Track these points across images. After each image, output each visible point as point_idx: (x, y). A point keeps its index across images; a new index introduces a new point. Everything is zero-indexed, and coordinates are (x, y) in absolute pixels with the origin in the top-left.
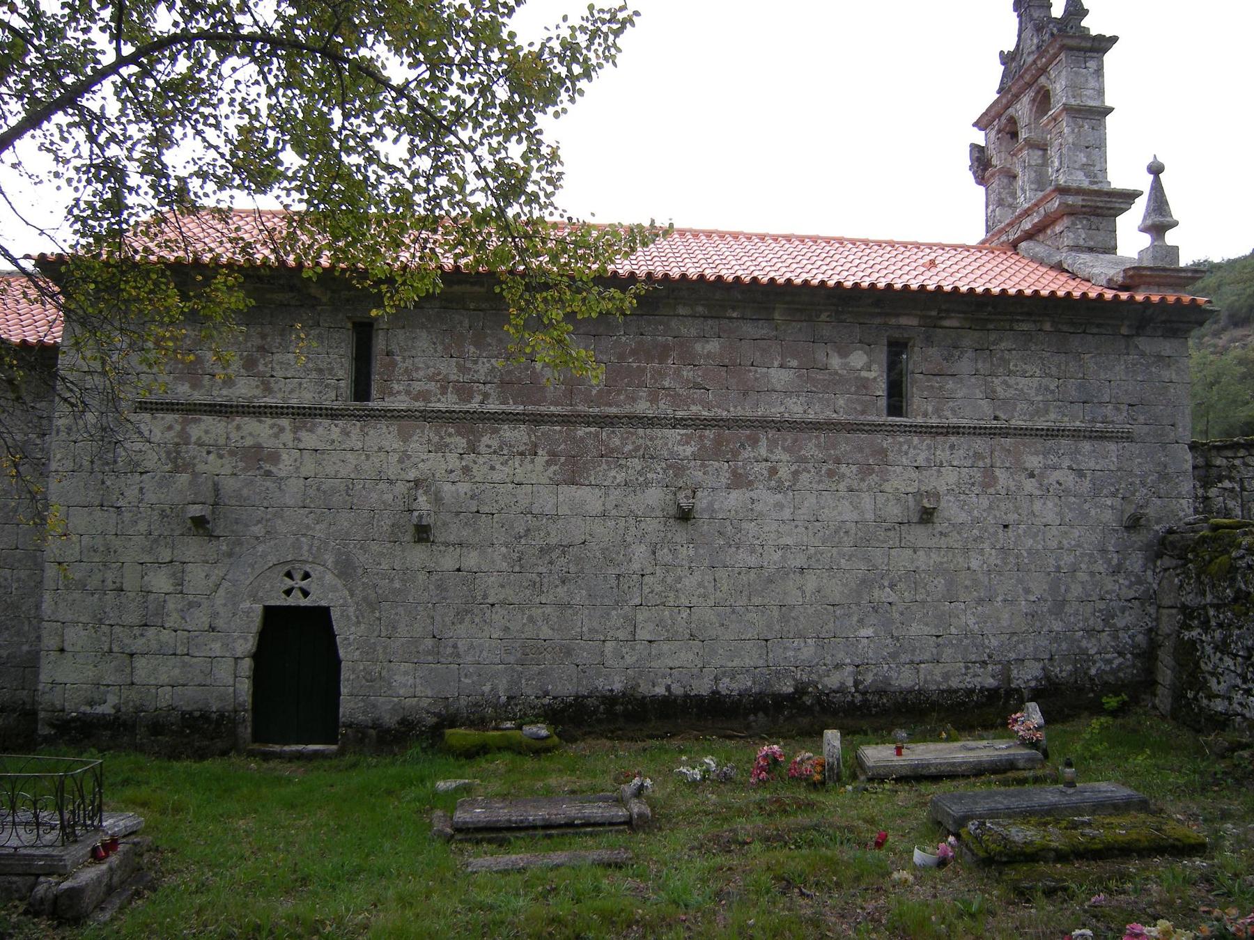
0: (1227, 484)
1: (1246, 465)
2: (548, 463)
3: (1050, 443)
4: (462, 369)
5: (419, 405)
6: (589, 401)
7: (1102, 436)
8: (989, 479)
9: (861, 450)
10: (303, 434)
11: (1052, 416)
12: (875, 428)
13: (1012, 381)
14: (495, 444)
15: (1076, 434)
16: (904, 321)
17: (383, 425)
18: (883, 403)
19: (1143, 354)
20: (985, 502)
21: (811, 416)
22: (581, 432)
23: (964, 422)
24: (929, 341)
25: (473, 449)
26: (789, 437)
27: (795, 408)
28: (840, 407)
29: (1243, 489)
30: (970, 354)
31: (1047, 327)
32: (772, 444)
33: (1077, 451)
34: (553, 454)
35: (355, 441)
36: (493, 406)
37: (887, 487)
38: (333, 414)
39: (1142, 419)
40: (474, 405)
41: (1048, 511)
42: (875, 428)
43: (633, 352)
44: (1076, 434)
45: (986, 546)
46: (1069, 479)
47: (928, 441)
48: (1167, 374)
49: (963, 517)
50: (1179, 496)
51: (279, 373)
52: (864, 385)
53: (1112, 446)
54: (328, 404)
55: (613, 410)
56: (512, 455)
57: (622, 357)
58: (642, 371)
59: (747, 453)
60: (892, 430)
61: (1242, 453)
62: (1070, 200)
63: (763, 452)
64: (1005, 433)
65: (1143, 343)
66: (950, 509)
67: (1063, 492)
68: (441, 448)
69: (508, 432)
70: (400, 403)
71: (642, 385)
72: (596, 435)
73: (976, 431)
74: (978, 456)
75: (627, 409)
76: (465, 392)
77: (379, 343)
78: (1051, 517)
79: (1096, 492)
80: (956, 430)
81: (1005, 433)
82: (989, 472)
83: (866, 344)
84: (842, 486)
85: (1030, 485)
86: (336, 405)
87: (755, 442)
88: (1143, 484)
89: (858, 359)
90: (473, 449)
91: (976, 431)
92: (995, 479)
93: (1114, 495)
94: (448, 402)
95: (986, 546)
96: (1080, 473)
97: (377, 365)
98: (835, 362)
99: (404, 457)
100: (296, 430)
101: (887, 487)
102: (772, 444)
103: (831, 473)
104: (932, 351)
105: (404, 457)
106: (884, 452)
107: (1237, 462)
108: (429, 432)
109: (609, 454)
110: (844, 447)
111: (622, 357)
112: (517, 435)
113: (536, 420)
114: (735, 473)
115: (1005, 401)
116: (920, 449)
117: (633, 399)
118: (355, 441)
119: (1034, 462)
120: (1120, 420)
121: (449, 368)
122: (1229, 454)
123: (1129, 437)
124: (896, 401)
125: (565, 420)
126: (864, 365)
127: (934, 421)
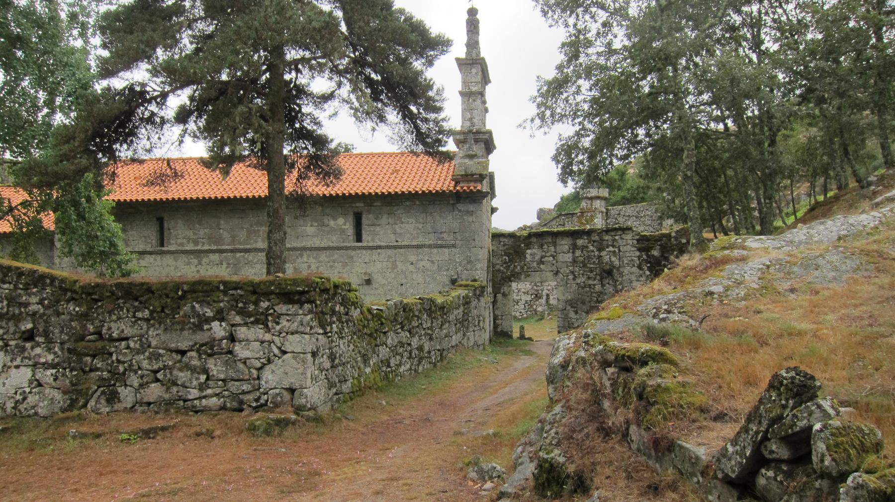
0: (611, 249)
1: (622, 239)
2: (227, 268)
3: (420, 250)
4: (195, 234)
5: (180, 248)
6: (240, 244)
7: (441, 246)
8: (394, 266)
9: (343, 257)
10: (141, 261)
11: (420, 239)
12: (347, 248)
13: (403, 226)
14: (208, 261)
15: (430, 246)
16: (358, 205)
17: (168, 256)
18: (351, 238)
19: (460, 211)
20: (393, 276)
21: (322, 245)
22: (238, 255)
23: (383, 244)
24: (369, 212)
25: (200, 263)
26: (315, 253)
27: (317, 242)
28: (334, 240)
29: (620, 251)
30: (385, 216)
31: (417, 203)
32: (309, 256)
33: (431, 253)
34: (228, 264)
35: (159, 262)
36: (206, 247)
37: (354, 271)
38: (151, 253)
39: (459, 238)
40: (199, 247)
41: (419, 278)
42: (347, 248)
43: (256, 224)
44: (430, 246)
45: (393, 292)
46: (428, 265)
47: (369, 252)
48: (470, 219)
49: (384, 282)
50: (476, 269)
51: (131, 239)
52: (343, 231)
53: (446, 250)
54: (148, 250)
55: (248, 247)
56: (214, 265)
57: (251, 226)
58: (259, 231)
59: (299, 260)
60: (354, 248)
61: (619, 233)
62: (458, 137)
63: (305, 260)
64: (400, 247)
65: (461, 206)
66: (378, 279)
67: (425, 270)
68: (189, 264)
69: (213, 257)
70: (172, 248)
71: (259, 236)
72: (243, 256)
73: (388, 247)
74: (389, 257)
75: (254, 246)
76: (196, 243)
77: (166, 226)
78: (420, 280)
79: (440, 269)
80: (380, 247)
81: (400, 247)
82: (394, 264)
83: (345, 215)
84: (336, 271)
85: (411, 268)
86: (151, 250)
87: (301, 256)
88: (460, 265)
89: (341, 221)
90: (200, 263)
91: (388, 247)
92: (396, 266)
93: (448, 270)
94: (190, 247)
95: (393, 292)
96: (433, 262)
97: (166, 233)
98: (332, 223)
99: (176, 268)
100: (138, 259)
101: (354, 271)
102: (309, 256)
103: (331, 267)
104: (371, 216)
105: (176, 268)
106: (352, 257)
107: (617, 238)
108: (183, 258)
109: (248, 263)
110: (336, 256)
111: (251, 226)
112: (215, 257)
113: (221, 251)
114: (295, 268)
115: (400, 234)
116: (366, 255)
117: (256, 242)
118: (159, 262)
119: (413, 258)
120: (449, 239)
121: (190, 233)
122: (613, 234)
123: (454, 246)
124: (359, 238)
125: (232, 251)
126: (345, 224)
127: (371, 244)
